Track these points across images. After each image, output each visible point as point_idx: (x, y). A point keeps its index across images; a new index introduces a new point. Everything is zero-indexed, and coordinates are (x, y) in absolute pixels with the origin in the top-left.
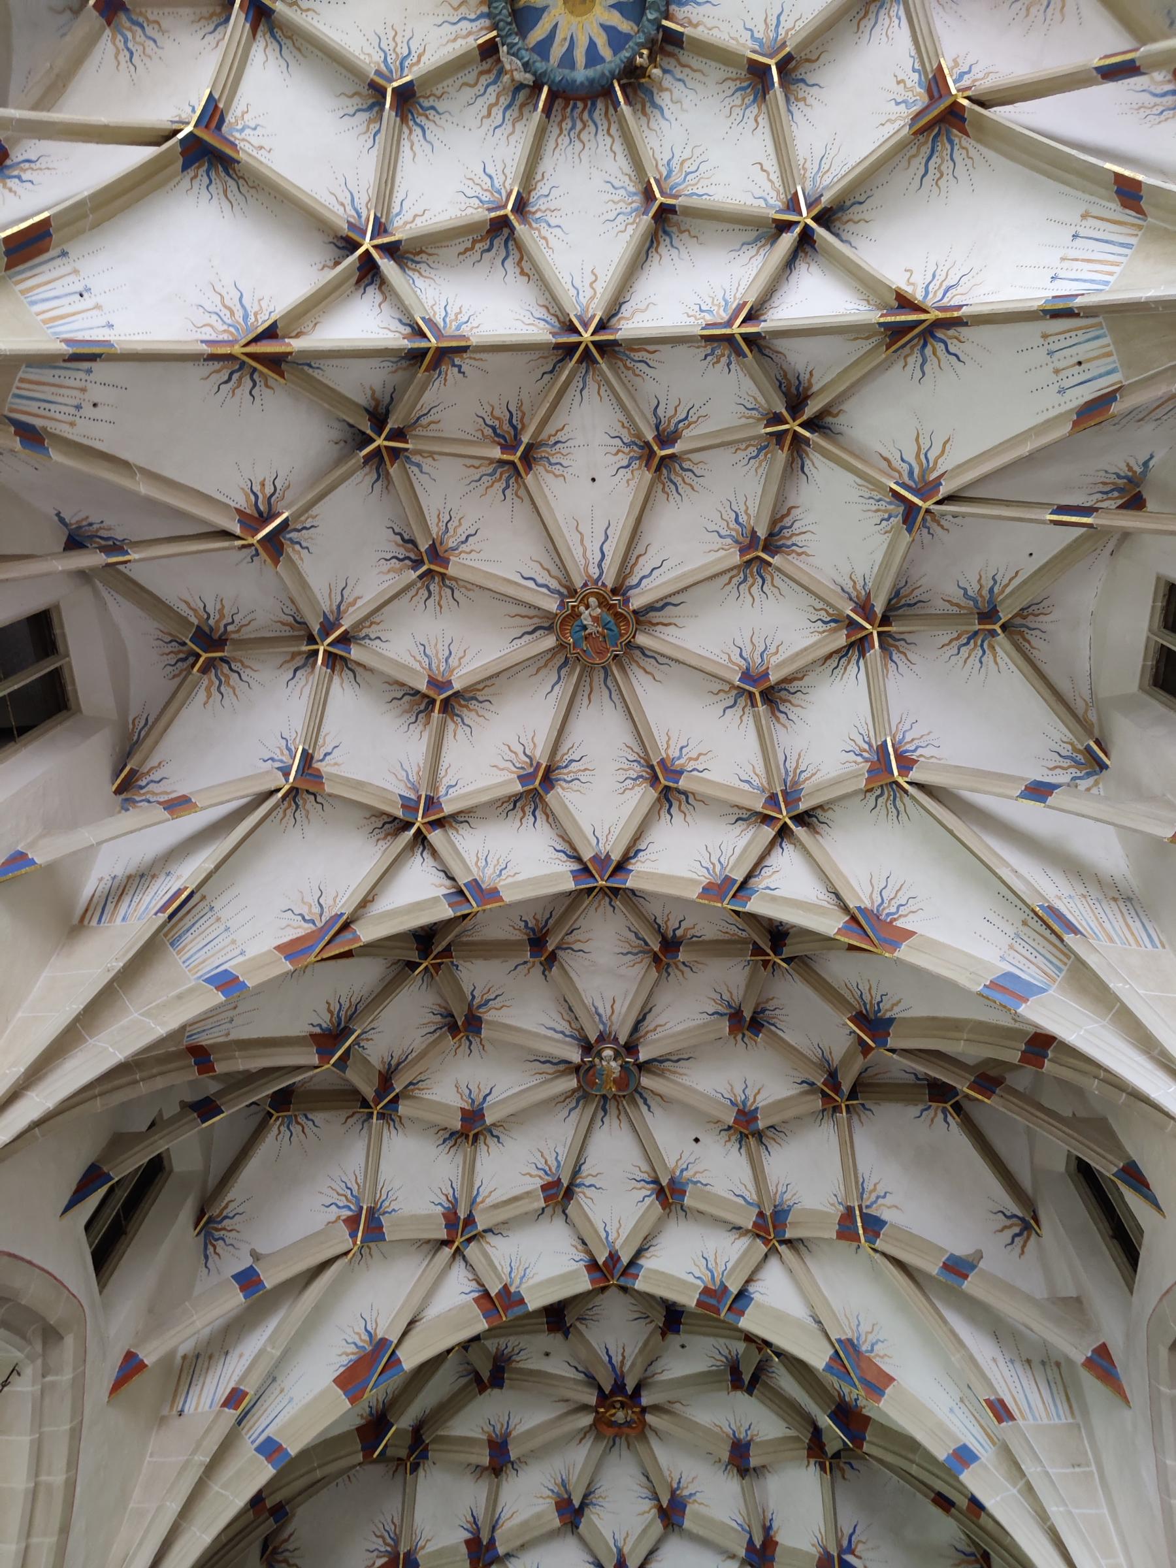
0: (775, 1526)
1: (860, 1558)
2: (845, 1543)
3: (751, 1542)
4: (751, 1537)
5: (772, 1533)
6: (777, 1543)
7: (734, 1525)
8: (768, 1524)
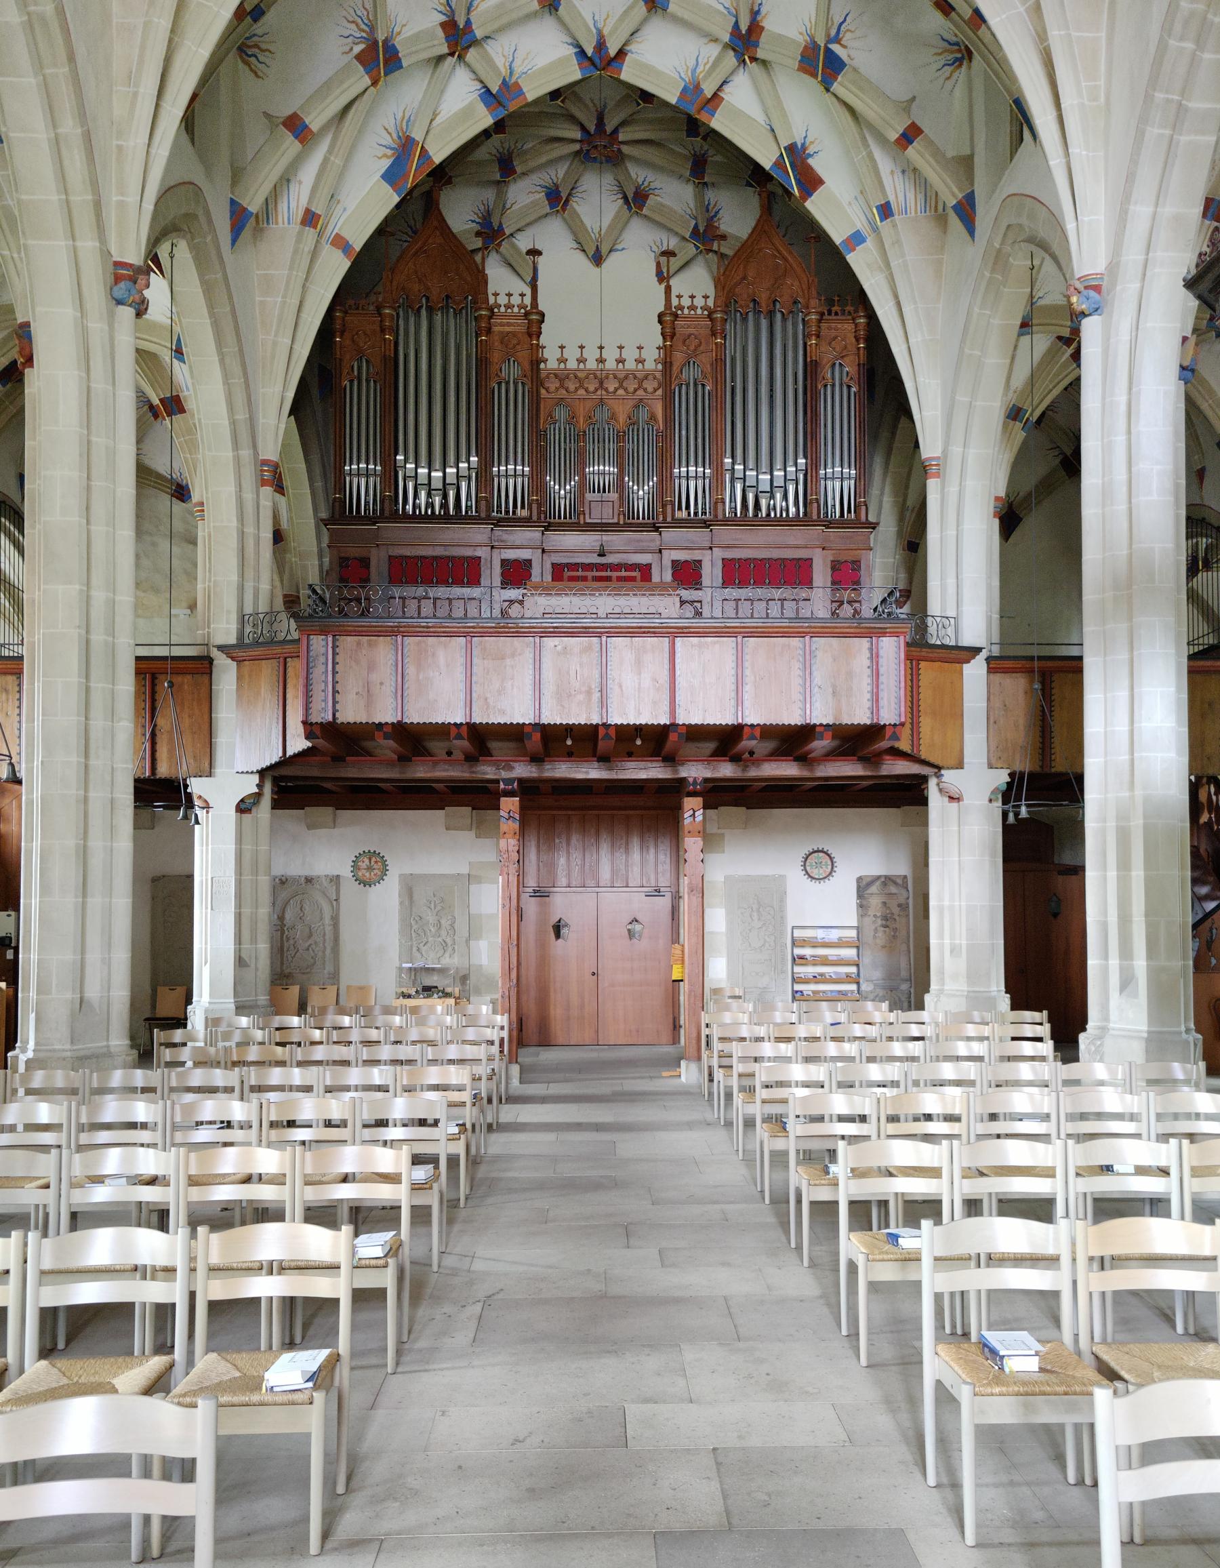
0: (764, 10)
1: (844, 47)
2: (833, 32)
4: (737, 23)
5: (759, 18)
6: (763, 28)
7: (721, 8)
8: (756, 8)
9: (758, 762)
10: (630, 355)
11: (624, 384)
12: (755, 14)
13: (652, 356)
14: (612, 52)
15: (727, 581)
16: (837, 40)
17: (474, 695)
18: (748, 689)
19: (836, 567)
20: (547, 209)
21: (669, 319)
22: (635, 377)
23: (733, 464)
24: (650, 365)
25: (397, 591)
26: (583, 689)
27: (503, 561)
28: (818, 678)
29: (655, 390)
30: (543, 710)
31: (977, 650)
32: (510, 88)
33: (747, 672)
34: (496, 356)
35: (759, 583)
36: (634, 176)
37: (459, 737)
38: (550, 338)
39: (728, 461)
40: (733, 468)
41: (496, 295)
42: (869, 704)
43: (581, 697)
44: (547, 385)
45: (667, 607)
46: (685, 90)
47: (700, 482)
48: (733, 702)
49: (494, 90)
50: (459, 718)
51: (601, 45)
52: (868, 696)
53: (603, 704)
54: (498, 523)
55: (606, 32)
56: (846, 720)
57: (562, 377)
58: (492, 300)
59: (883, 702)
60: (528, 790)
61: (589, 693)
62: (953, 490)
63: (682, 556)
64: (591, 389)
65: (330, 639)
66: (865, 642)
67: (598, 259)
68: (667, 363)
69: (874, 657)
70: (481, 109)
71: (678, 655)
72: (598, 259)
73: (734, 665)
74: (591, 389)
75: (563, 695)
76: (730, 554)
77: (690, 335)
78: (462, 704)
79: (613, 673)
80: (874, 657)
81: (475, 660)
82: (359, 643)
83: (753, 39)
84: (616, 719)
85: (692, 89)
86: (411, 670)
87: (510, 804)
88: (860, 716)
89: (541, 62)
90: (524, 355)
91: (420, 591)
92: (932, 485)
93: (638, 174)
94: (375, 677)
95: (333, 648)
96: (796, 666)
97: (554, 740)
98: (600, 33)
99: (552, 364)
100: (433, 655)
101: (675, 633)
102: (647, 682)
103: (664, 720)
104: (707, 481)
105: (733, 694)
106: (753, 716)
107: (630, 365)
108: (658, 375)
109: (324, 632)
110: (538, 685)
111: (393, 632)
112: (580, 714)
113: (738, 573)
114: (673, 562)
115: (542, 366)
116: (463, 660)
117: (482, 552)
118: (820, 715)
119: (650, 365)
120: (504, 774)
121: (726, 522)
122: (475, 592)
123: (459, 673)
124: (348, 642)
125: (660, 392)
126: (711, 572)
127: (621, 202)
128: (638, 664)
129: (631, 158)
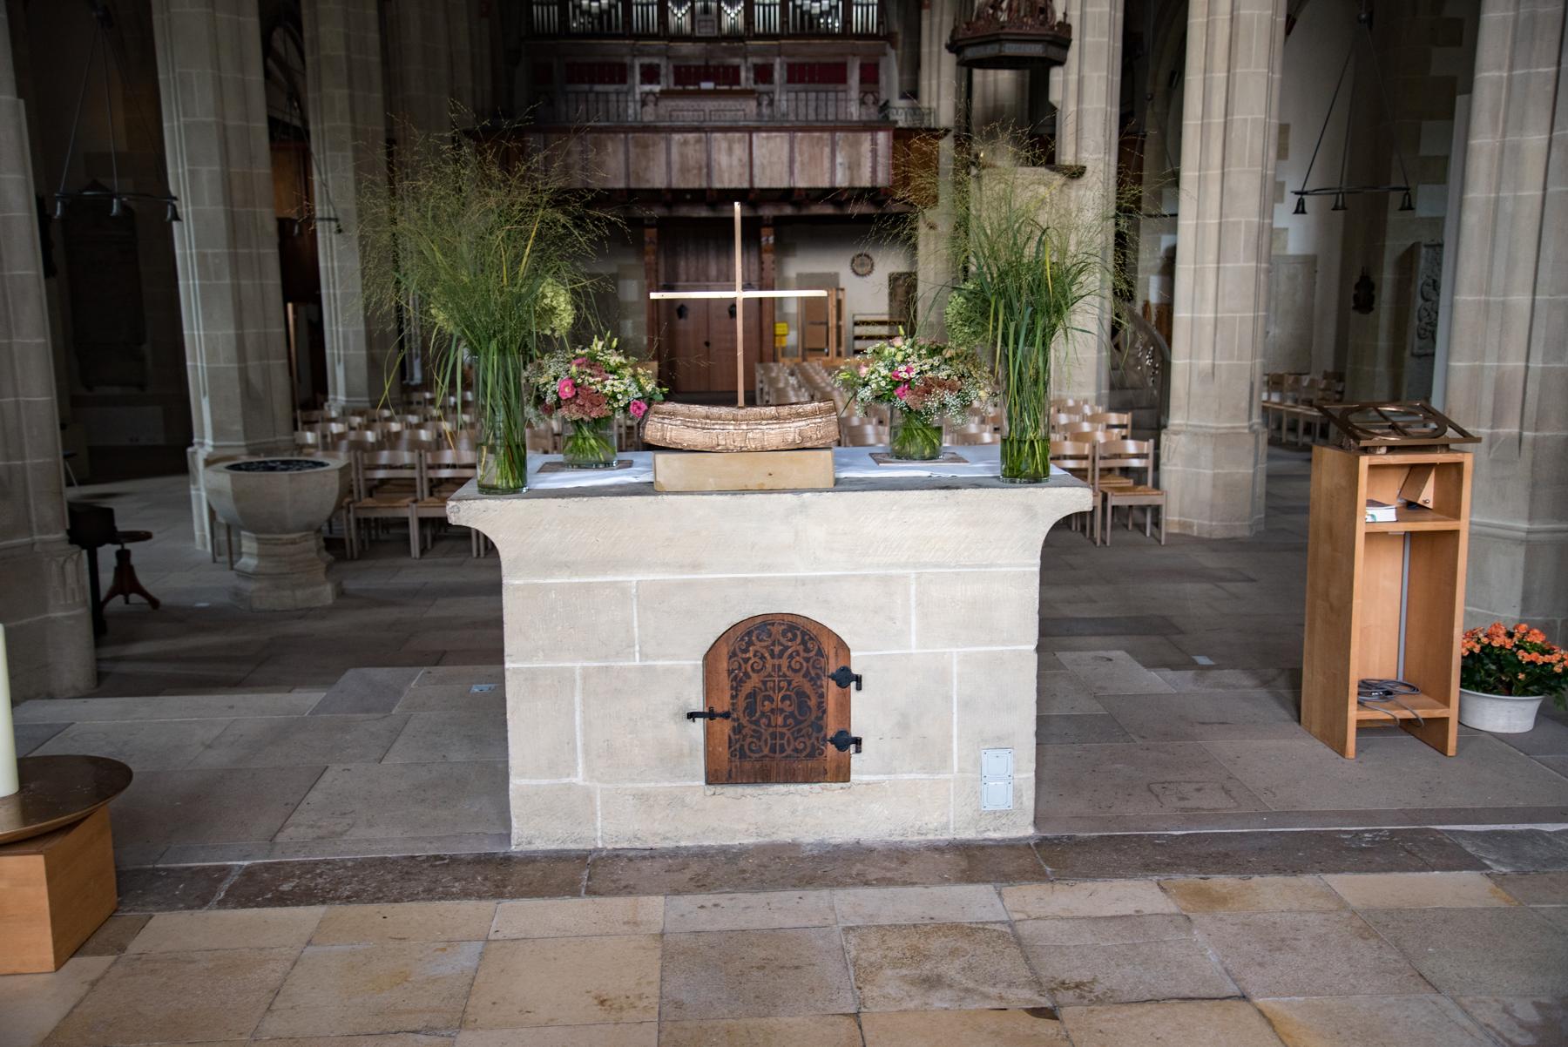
15: (790, 80)
18: (797, 165)
19: (863, 67)
25: (570, 87)
27: (642, 66)
28: (839, 160)
31: (947, 131)
50: (621, 185)
53: (709, 175)
54: (638, 37)
56: (857, 184)
60: (661, 223)
61: (700, 169)
62: (936, 20)
63: (758, 60)
69: (874, 142)
75: (684, 170)
76: (792, 60)
79: (714, 155)
80: (874, 142)
84: (717, 185)
87: (651, 234)
88: (865, 181)
91: (586, 87)
92: (925, 13)
94: (570, 161)
96: (827, 150)
101: (751, 130)
102: (735, 162)
103: (746, 185)
106: (801, 183)
113: (797, 74)
114: (755, 65)
117: (627, 60)
118: (841, 181)
121: (789, 37)
122: (625, 87)
123: (621, 157)
128: (730, 150)
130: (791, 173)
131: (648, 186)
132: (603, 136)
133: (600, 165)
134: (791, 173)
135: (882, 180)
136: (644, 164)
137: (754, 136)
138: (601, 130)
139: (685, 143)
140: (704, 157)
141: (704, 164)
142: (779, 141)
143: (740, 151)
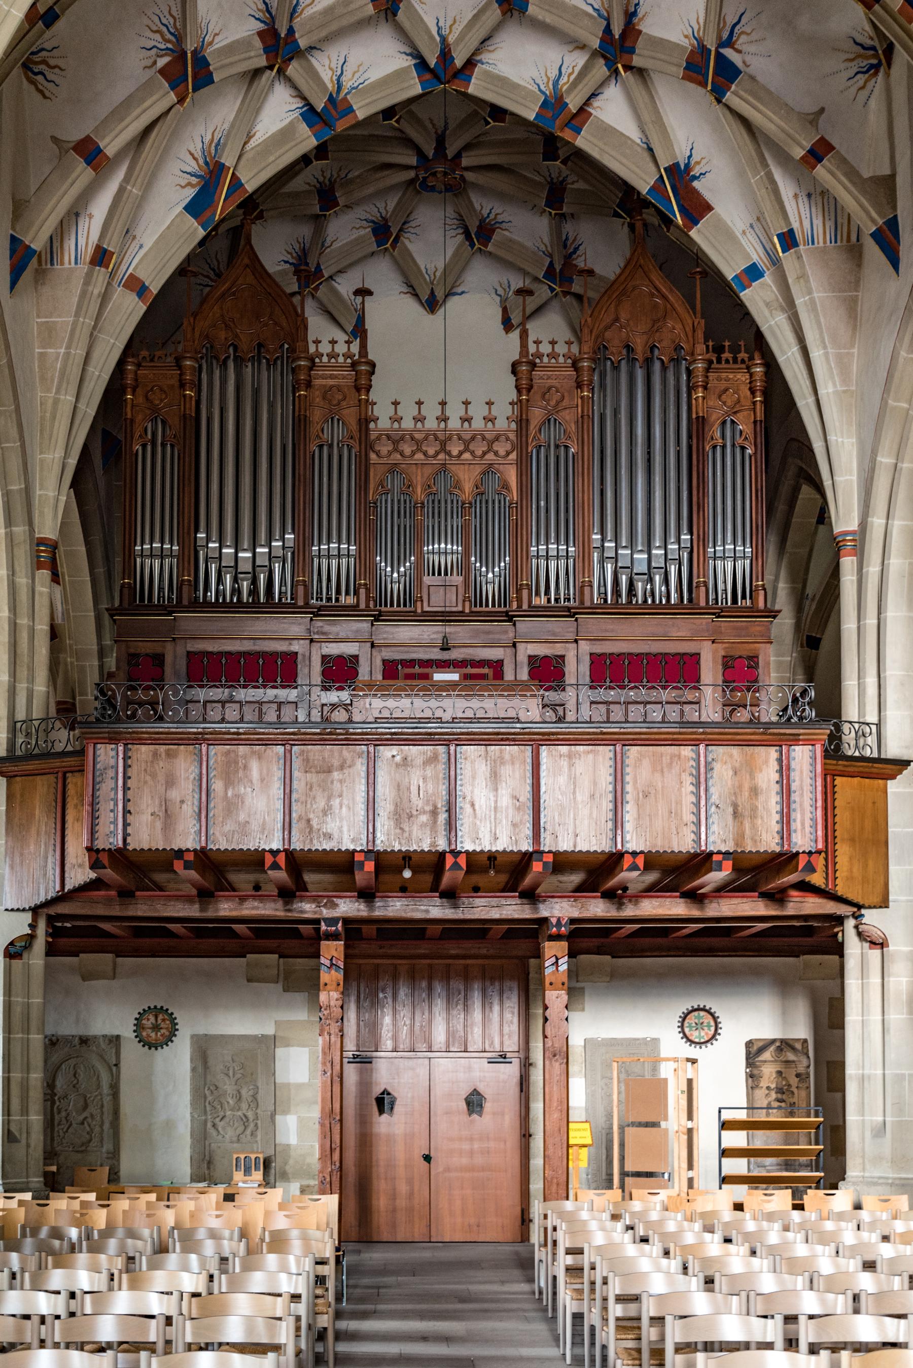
0: (641, 12)
1: (739, 51)
2: (725, 35)
3: (608, 30)
5: (635, 20)
6: (640, 32)
7: (590, 10)
9: (636, 899)
10: (478, 412)
11: (471, 447)
12: (630, 16)
13: (503, 412)
14: (459, 63)
16: (729, 43)
17: (294, 815)
20: (374, 247)
21: (524, 370)
22: (484, 438)
23: (603, 540)
24: (502, 424)
26: (428, 808)
29: (508, 453)
30: (378, 834)
32: (338, 104)
33: (629, 788)
34: (317, 415)
35: (636, 678)
36: (477, 206)
37: (275, 866)
38: (381, 396)
39: (597, 537)
40: (603, 546)
41: (317, 342)
42: (777, 827)
43: (424, 818)
44: (377, 448)
45: (529, 709)
46: (545, 104)
47: (562, 562)
48: (610, 825)
49: (320, 106)
51: (445, 54)
52: (777, 817)
53: (451, 826)
55: (451, 39)
57: (396, 440)
58: (312, 349)
59: (796, 825)
61: (434, 813)
62: (873, 570)
64: (431, 452)
65: (121, 748)
66: (773, 753)
67: (432, 304)
68: (522, 422)
69: (784, 769)
70: (304, 129)
71: (543, 768)
72: (432, 304)
73: (611, 779)
74: (431, 452)
77: (549, 389)
78: (280, 825)
79: (465, 788)
80: (784, 769)
81: (296, 774)
82: (155, 754)
83: (628, 44)
84: (467, 845)
85: (554, 104)
86: (218, 786)
87: (332, 950)
88: (767, 840)
89: (374, 75)
90: (350, 415)
93: (483, 205)
94: (174, 795)
95: (124, 759)
96: (688, 780)
97: (390, 870)
98: (444, 39)
99: (384, 423)
100: (245, 767)
101: (536, 740)
102: (505, 800)
103: (526, 846)
104: (571, 561)
105: (611, 815)
106: (634, 841)
107: (478, 424)
108: (512, 436)
109: (113, 739)
110: (371, 804)
111: (197, 739)
112: (423, 839)
115: (372, 425)
116: (280, 774)
119: (502, 424)
120: (326, 913)
123: (276, 789)
124: (143, 752)
125: (513, 456)
126: (577, 668)
127: (461, 238)
128: (495, 777)
129: (475, 185)
130: (617, 822)
131: (327, 846)
132: (242, 750)
133: (231, 807)
134: (617, 822)
135: (804, 839)
136: (321, 803)
137: (544, 751)
138: (236, 739)
139: (405, 762)
140: (443, 789)
141: (441, 804)
142: (594, 764)
143: (515, 778)
